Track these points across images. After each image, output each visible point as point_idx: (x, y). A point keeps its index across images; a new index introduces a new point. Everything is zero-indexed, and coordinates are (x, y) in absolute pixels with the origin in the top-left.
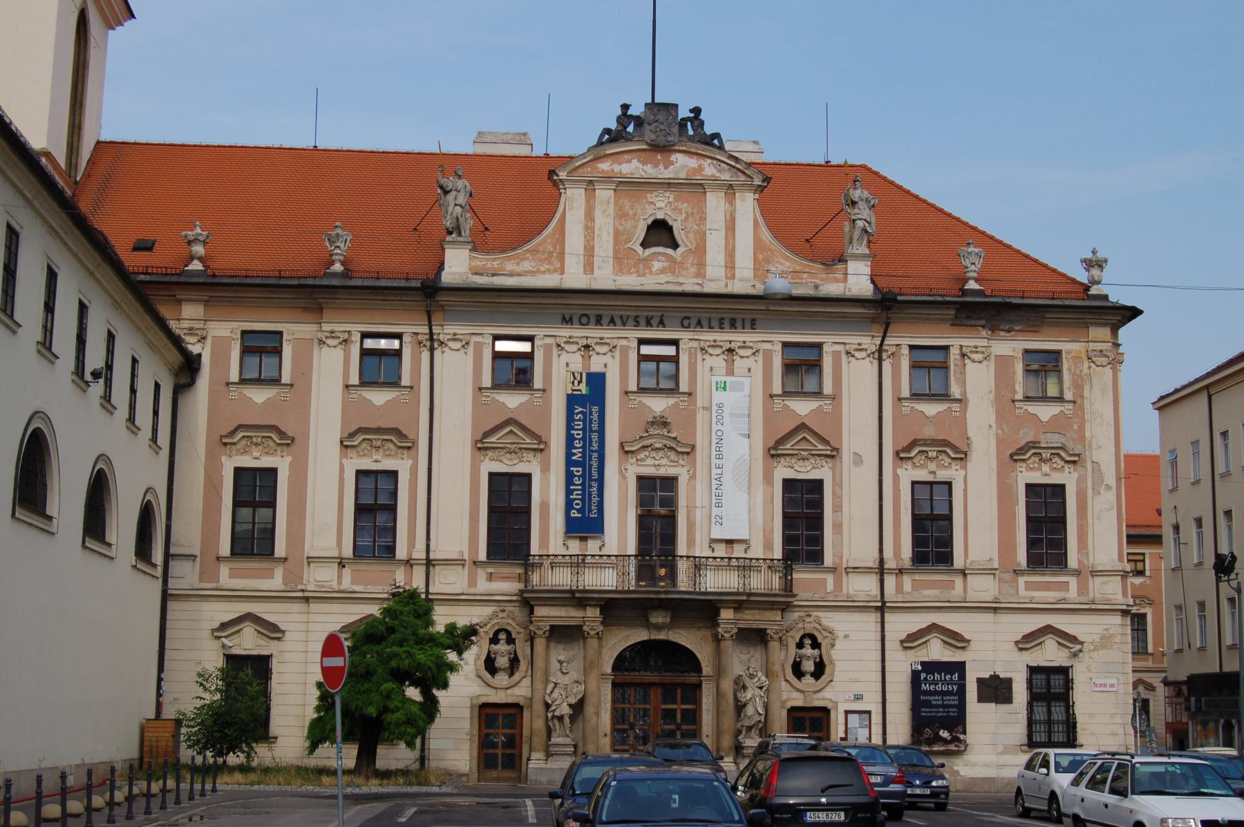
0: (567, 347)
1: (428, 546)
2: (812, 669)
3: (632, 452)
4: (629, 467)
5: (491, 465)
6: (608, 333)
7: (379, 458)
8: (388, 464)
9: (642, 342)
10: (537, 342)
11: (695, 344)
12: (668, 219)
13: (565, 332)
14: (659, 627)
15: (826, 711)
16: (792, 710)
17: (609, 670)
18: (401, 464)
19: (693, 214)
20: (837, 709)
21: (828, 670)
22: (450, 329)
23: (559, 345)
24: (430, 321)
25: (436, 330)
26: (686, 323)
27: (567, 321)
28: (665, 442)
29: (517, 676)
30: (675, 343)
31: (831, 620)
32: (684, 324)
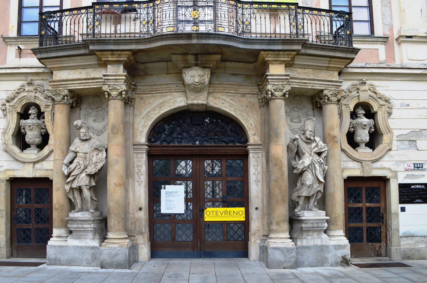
2: (367, 139)
14: (197, 89)
15: (384, 181)
16: (349, 180)
17: (142, 139)
20: (396, 177)
21: (386, 138)
29: (46, 150)
31: (384, 87)
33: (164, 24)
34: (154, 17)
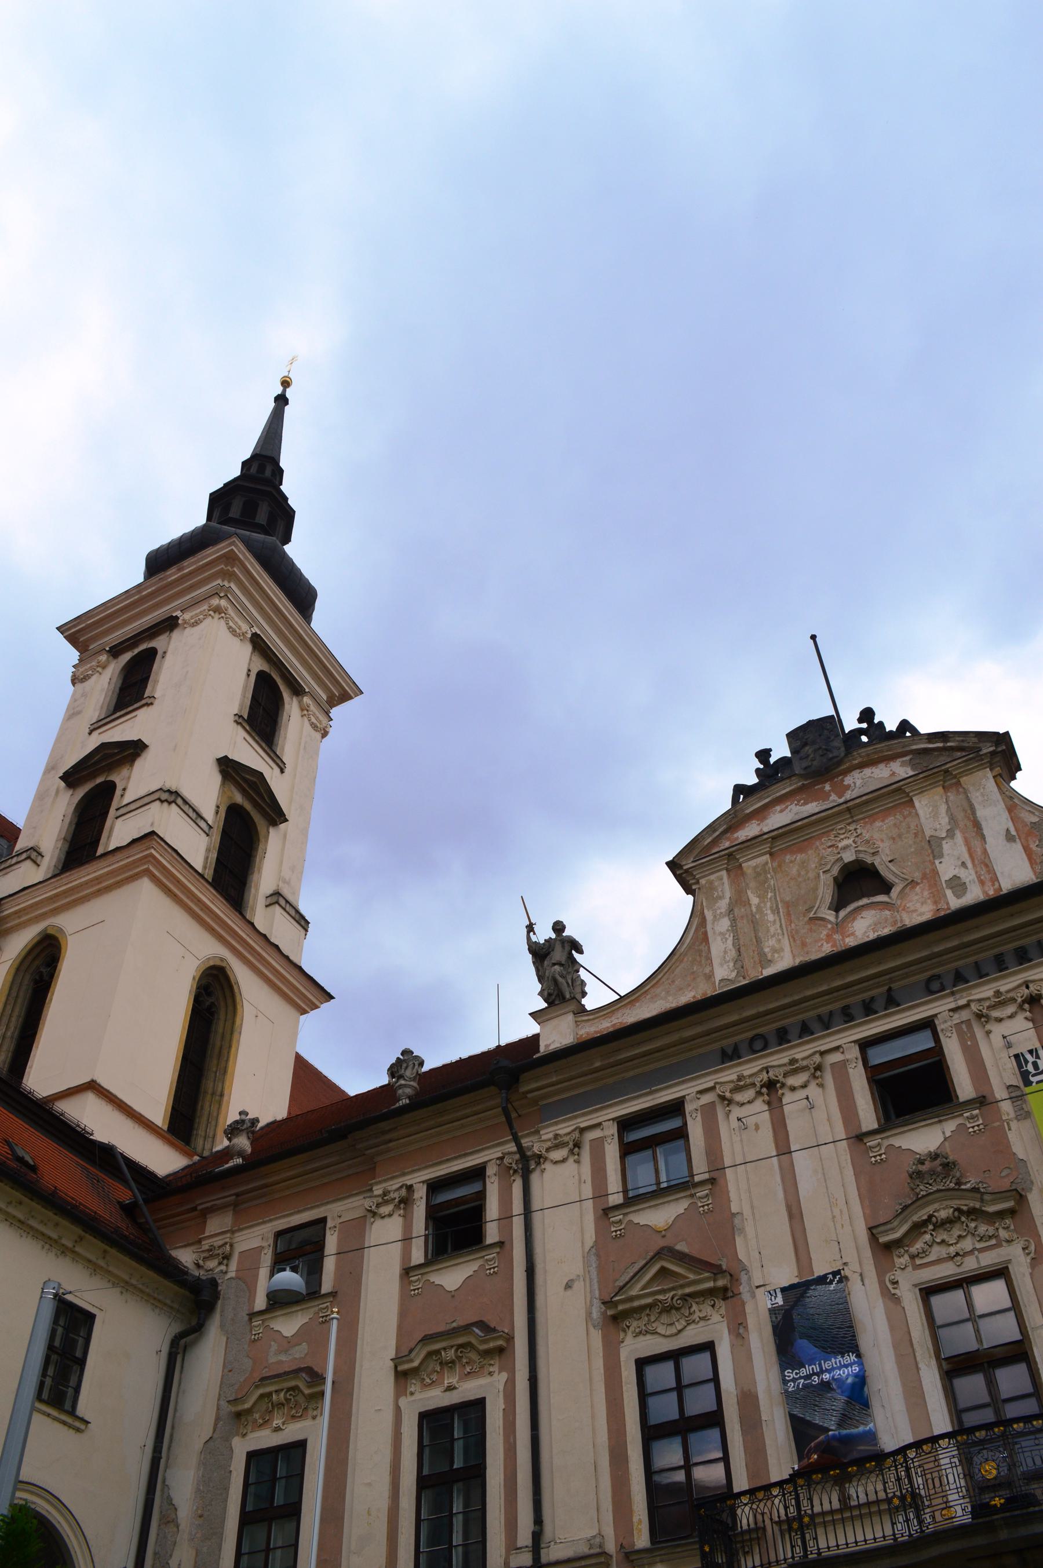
0: (739, 1097)
1: (537, 1536)
3: (898, 1243)
4: (899, 1275)
5: (635, 1346)
6: (802, 1052)
7: (453, 1380)
8: (468, 1389)
9: (865, 1045)
10: (689, 1107)
11: (965, 1015)
12: (861, 856)
13: (729, 1075)
18: (486, 1385)
19: (900, 836)
22: (547, 1134)
23: (723, 1098)
24: (511, 1127)
25: (525, 1142)
26: (935, 985)
27: (730, 1056)
28: (956, 1203)
30: (928, 1024)
32: (933, 987)
33: (934, 1502)
34: (911, 1487)
